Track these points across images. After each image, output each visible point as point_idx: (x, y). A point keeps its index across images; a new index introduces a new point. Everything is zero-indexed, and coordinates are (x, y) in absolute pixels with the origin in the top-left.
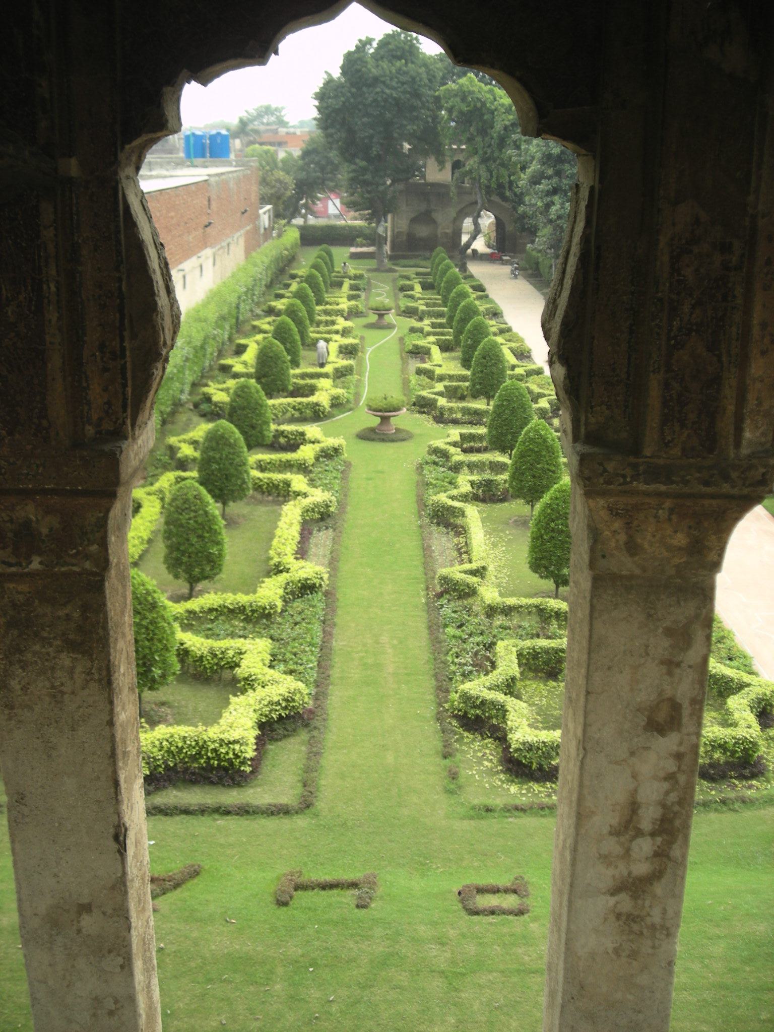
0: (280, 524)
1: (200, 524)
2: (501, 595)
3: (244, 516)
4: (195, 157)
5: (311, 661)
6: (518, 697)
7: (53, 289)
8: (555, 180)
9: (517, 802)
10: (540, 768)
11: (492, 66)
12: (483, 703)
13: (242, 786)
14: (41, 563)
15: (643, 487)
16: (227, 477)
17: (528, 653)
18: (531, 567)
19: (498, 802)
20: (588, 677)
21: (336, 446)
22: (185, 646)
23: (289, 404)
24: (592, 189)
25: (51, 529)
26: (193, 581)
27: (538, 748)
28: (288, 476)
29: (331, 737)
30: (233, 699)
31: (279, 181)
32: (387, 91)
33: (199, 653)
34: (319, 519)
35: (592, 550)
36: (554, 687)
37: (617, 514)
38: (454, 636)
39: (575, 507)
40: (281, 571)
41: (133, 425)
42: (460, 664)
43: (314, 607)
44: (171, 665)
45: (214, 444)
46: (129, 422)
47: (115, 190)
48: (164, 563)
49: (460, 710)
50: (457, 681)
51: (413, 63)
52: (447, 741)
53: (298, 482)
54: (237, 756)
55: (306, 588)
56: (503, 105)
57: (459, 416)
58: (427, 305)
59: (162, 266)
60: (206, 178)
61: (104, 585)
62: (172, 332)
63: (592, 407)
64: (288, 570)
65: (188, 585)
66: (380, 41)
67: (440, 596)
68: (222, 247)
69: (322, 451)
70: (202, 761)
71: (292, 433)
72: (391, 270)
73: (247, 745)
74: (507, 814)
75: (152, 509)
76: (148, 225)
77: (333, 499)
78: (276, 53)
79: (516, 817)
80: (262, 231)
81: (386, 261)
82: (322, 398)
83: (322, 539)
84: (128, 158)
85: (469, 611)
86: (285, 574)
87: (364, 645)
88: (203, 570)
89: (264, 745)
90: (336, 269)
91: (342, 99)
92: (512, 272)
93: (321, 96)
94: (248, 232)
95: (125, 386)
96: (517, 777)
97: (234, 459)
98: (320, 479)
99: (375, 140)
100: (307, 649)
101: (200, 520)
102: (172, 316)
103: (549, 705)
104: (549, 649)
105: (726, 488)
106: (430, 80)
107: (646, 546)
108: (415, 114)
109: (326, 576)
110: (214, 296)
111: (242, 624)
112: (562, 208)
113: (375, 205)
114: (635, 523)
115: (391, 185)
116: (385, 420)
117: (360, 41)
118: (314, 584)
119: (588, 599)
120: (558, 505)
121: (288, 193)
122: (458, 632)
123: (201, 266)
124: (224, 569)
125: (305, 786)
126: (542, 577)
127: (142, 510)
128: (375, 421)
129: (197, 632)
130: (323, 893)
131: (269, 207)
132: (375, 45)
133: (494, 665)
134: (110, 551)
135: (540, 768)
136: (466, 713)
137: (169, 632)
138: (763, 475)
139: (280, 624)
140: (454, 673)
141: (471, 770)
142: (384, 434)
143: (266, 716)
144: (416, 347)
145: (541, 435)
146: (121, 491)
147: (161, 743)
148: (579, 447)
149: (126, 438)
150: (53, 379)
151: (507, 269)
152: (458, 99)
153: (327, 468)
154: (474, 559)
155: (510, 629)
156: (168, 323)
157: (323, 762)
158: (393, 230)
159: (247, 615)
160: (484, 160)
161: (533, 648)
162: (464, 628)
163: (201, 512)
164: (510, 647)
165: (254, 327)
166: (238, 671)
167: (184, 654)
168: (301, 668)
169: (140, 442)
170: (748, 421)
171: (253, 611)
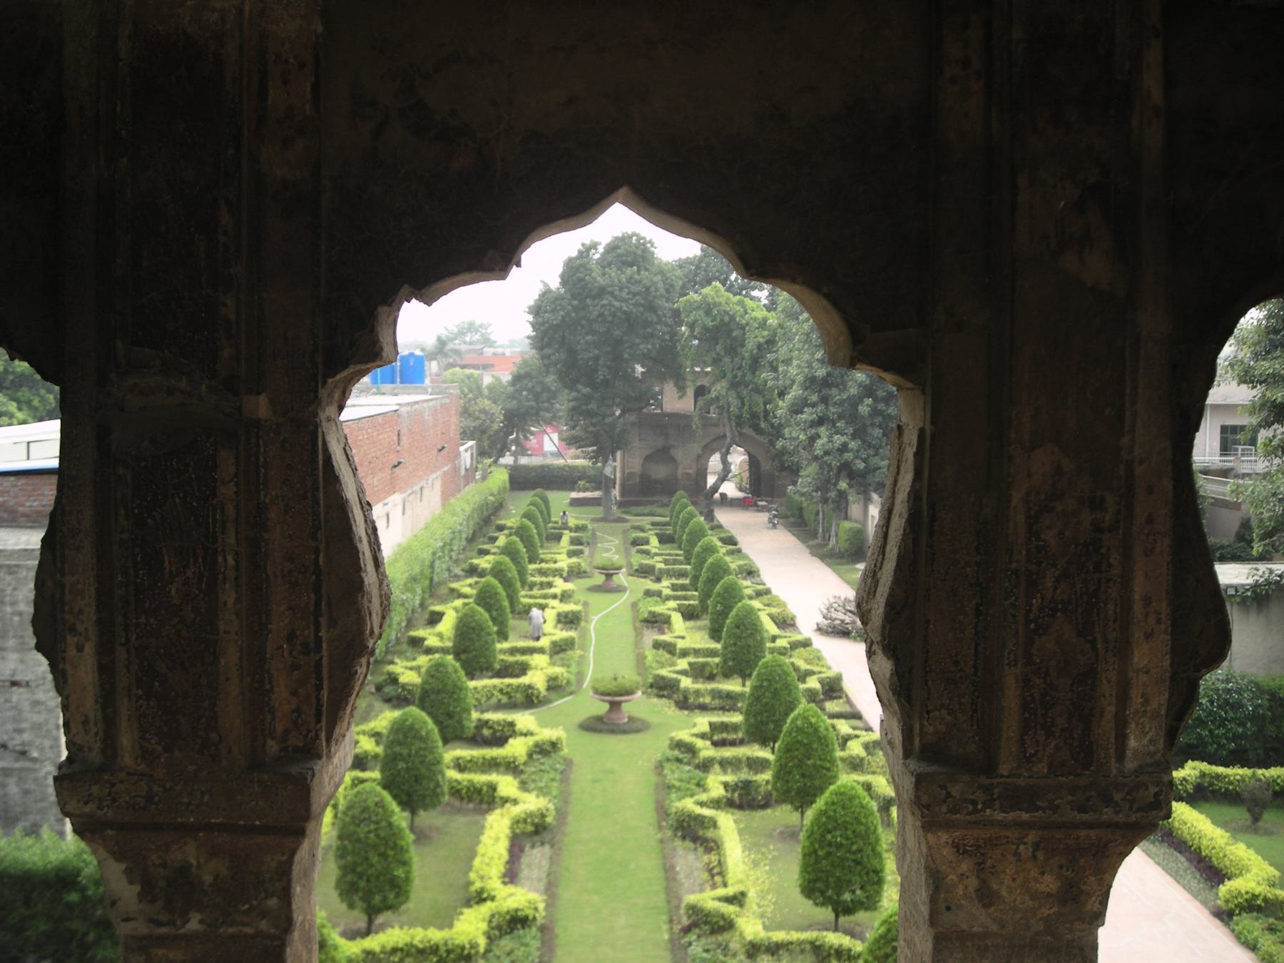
0: (484, 838)
1: (384, 838)
2: (766, 928)
3: (437, 829)
7: (231, 561)
8: (821, 408)
11: (793, 280)
14: (201, 922)
15: (1000, 816)
16: (417, 779)
18: (803, 892)
21: (554, 739)
23: (495, 687)
24: (922, 433)
25: (217, 876)
26: (372, 912)
28: (493, 777)
31: (486, 413)
32: (617, 304)
34: (532, 833)
35: (933, 900)
37: (965, 851)
40: (484, 900)
41: (329, 739)
43: (526, 945)
45: (401, 737)
46: (323, 735)
51: (646, 270)
53: (506, 785)
55: (516, 922)
56: (755, 319)
57: (707, 700)
59: (370, 532)
63: (928, 712)
64: (493, 899)
67: (687, 930)
69: (537, 745)
71: (498, 723)
77: (551, 806)
78: (518, 265)
80: (463, 472)
81: (615, 508)
82: (536, 678)
83: (536, 857)
84: (331, 395)
85: (725, 949)
86: (489, 904)
88: (385, 899)
90: (553, 519)
92: (770, 521)
93: (537, 310)
94: (445, 473)
95: (319, 688)
98: (534, 781)
99: (601, 362)
101: (382, 834)
102: (381, 596)
105: (1107, 814)
106: (668, 291)
107: (1004, 893)
108: (649, 330)
113: (603, 442)
114: (989, 863)
115: (620, 416)
116: (615, 706)
117: (583, 245)
120: (835, 811)
121: (495, 427)
124: (413, 896)
126: (817, 904)
128: (602, 708)
131: (471, 443)
132: (601, 249)
134: (294, 907)
138: (1156, 795)
144: (653, 614)
146: (311, 826)
148: (913, 764)
149: (320, 757)
150: (227, 679)
151: (764, 517)
152: (701, 312)
154: (730, 882)
158: (623, 472)
160: (734, 385)
165: (452, 590)
169: (336, 760)
170: (1133, 725)
171: (449, 952)
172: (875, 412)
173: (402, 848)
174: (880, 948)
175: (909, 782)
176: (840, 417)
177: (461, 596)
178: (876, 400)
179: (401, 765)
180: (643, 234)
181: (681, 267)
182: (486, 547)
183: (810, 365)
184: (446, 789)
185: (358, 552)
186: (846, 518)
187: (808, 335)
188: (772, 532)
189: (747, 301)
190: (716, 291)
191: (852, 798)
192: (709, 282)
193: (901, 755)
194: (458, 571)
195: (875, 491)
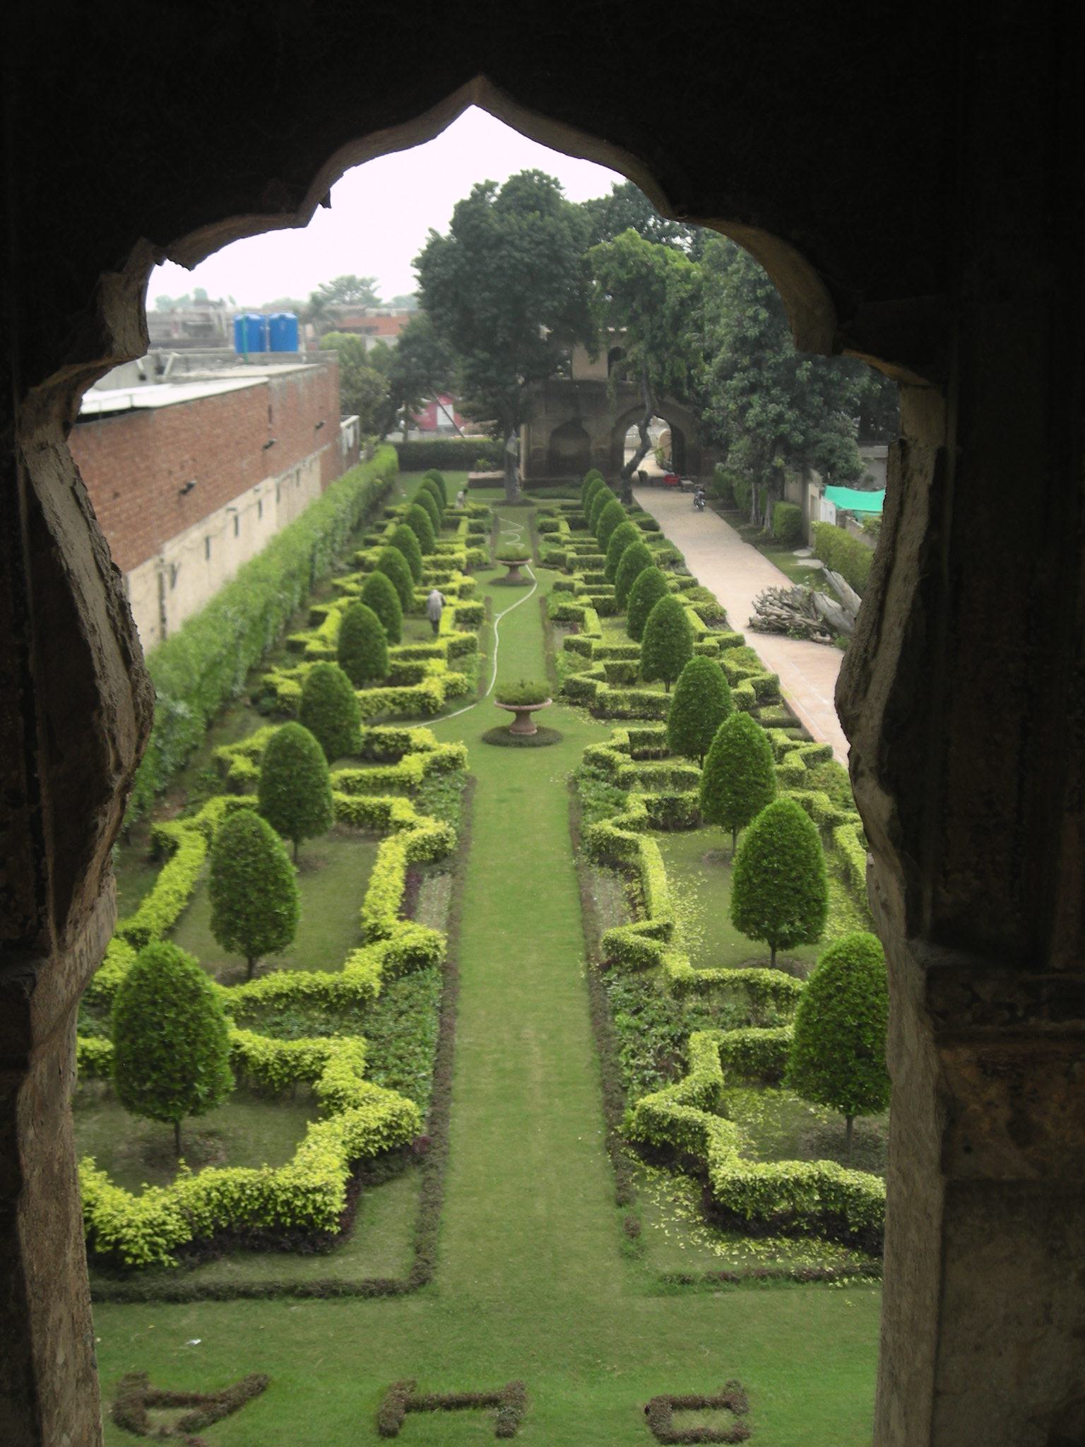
0: (377, 869)
1: (262, 873)
2: (694, 964)
3: (324, 858)
4: (250, 350)
5: (424, 1068)
6: (723, 1114)
8: (752, 373)
9: (726, 1268)
10: (758, 1217)
11: (746, 221)
12: (674, 1123)
13: (327, 1255)
15: (1047, 1025)
16: (300, 804)
17: (735, 1049)
18: (735, 924)
19: (698, 1269)
20: (937, 1363)
21: (454, 754)
22: (242, 1049)
23: (386, 696)
24: (941, 456)
26: (253, 954)
27: (754, 1189)
28: (387, 799)
29: (455, 1180)
30: (312, 1127)
31: (367, 381)
32: (517, 255)
33: (262, 1060)
34: (430, 861)
35: (946, 1139)
36: (774, 1097)
38: (628, 1027)
39: (900, 1037)
40: (379, 938)
41: (60, 926)
42: (638, 1067)
43: (426, 988)
44: (222, 1079)
45: (280, 756)
46: (51, 922)
47: (11, 475)
48: (212, 929)
49: (639, 1135)
50: (634, 1092)
51: (551, 215)
52: (622, 1180)
53: (401, 808)
54: (318, 1211)
55: (414, 961)
56: (677, 271)
57: (627, 707)
58: (578, 551)
59: (114, 613)
60: (266, 379)
62: (135, 738)
64: (388, 936)
65: (246, 961)
66: (505, 186)
67: (606, 968)
68: (289, 476)
70: (269, 1219)
71: (391, 737)
72: (526, 503)
73: (334, 1193)
74: (712, 1287)
75: (192, 850)
76: (85, 535)
77: (451, 830)
78: (326, 204)
79: (725, 1291)
80: (345, 452)
81: (519, 490)
82: (433, 686)
83: (436, 888)
85: (649, 988)
86: (384, 942)
88: (266, 938)
89: (358, 1192)
90: (450, 504)
91: (454, 266)
92: (696, 502)
93: (425, 263)
95: (39, 854)
96: (724, 1231)
97: (308, 778)
98: (432, 802)
99: (500, 322)
100: (418, 1050)
101: (261, 866)
102: (136, 705)
103: (766, 1122)
104: (764, 1042)
106: (575, 239)
108: (555, 285)
110: (278, 545)
111: (323, 1016)
112: (764, 411)
115: (524, 384)
116: (522, 716)
117: (477, 186)
118: (426, 956)
119: (936, 1222)
120: (771, 834)
121: (381, 399)
122: (634, 1021)
123: (260, 504)
124: (297, 935)
125: (418, 1252)
126: (751, 938)
127: (179, 852)
128: (508, 718)
129: (258, 1029)
130: (447, 1414)
131: (354, 418)
132: (498, 191)
133: (687, 1069)
134: (24, 1160)
135: (758, 1217)
136: (648, 1139)
137: (218, 1031)
139: (378, 1014)
140: (630, 1080)
141: (658, 1222)
142: (521, 736)
143: (360, 1150)
145: (744, 734)
147: (209, 1194)
149: (46, 952)
151: (689, 498)
152: (615, 264)
153: (442, 787)
154: (654, 913)
155: (708, 1014)
156: (124, 723)
157: (444, 1216)
158: (528, 448)
159: (331, 1002)
160: (653, 348)
161: (743, 1042)
162: (642, 1014)
163: (262, 856)
164: (709, 1041)
165: (336, 587)
166: (318, 1085)
167: (241, 1060)
168: (409, 1078)
169: (79, 945)
171: (339, 997)
172: (815, 377)
173: (284, 881)
174: (822, 989)
176: (776, 383)
177: (346, 593)
179: (282, 788)
180: (546, 173)
181: (590, 211)
182: (373, 537)
183: (740, 324)
185: (88, 650)
186: (783, 499)
187: (737, 288)
188: (699, 516)
189: (668, 250)
190: (629, 238)
191: (791, 819)
192: (622, 228)
193: (903, 930)
195: (815, 468)
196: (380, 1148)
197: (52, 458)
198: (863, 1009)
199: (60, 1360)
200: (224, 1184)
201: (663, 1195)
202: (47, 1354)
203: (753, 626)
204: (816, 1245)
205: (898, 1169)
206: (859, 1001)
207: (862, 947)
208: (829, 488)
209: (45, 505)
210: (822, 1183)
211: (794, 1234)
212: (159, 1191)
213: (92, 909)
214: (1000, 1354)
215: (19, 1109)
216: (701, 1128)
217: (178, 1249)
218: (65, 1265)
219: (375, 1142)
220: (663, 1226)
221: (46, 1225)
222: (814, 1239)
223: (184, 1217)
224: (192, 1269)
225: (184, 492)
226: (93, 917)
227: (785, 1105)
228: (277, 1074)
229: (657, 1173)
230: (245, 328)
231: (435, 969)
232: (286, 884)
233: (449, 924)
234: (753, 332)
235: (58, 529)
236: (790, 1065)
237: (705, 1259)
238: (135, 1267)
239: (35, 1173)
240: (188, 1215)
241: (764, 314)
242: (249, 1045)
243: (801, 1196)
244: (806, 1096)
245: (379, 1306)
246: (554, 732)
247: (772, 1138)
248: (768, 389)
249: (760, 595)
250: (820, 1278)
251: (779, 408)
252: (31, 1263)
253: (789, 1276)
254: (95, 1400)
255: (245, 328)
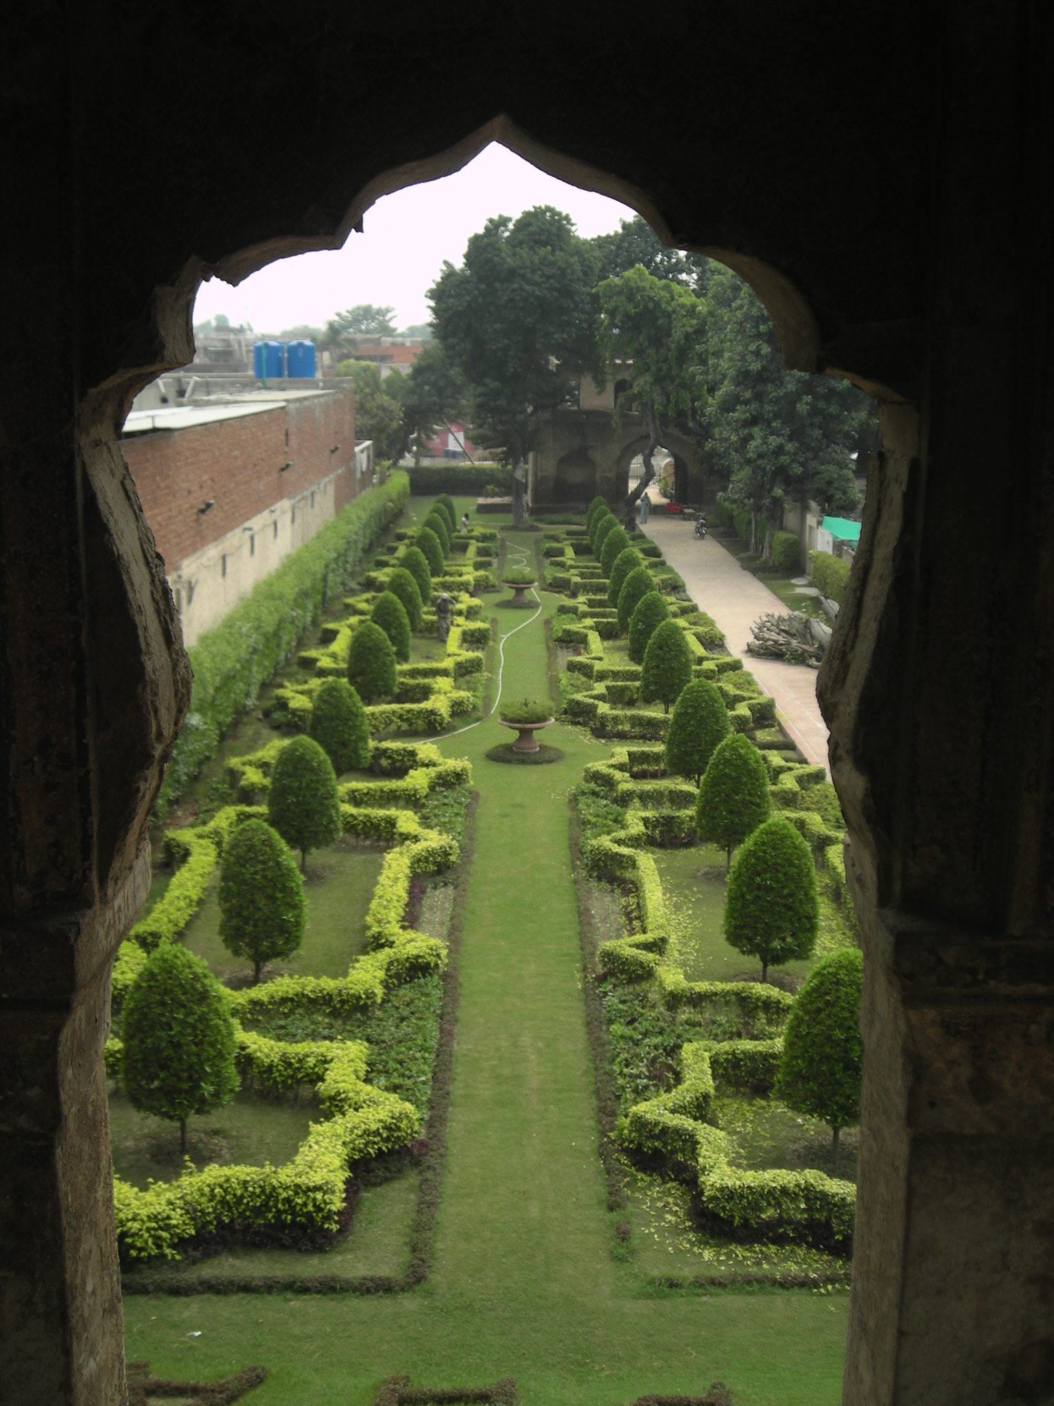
0: (381, 879)
1: (271, 880)
2: (688, 977)
3: (331, 868)
4: (268, 376)
5: (424, 1073)
6: (713, 1123)
9: (714, 1273)
10: (746, 1224)
11: (739, 249)
12: (665, 1130)
13: (326, 1252)
16: (309, 814)
17: (726, 1060)
18: (728, 939)
19: (687, 1273)
20: (902, 1305)
21: (459, 769)
22: (248, 1051)
24: (914, 466)
26: (259, 959)
27: (742, 1196)
28: (392, 812)
29: (451, 1181)
30: (314, 1128)
31: (382, 408)
32: (528, 288)
33: (267, 1061)
34: (432, 872)
35: (912, 1094)
36: (763, 1108)
38: (622, 1037)
39: (873, 1003)
40: (382, 946)
41: (103, 880)
42: (631, 1076)
43: (427, 995)
45: (291, 769)
46: (94, 876)
47: (69, 466)
48: (220, 934)
49: (631, 1142)
50: (626, 1100)
51: (561, 250)
52: (614, 1185)
53: (407, 821)
54: (318, 1209)
55: (416, 969)
56: (683, 306)
57: (627, 727)
58: (582, 575)
60: (283, 404)
61: (52, 1154)
62: (174, 711)
65: (253, 965)
66: (518, 221)
67: (602, 979)
68: (304, 498)
69: (439, 776)
70: (270, 1215)
71: (397, 752)
73: (333, 1192)
74: (700, 1291)
76: (133, 525)
78: (359, 229)
79: (711, 1295)
80: (359, 475)
81: (526, 515)
82: (439, 704)
83: (439, 899)
85: (644, 1000)
86: (387, 949)
87: (498, 1049)
88: (274, 944)
89: (357, 1192)
92: (698, 530)
94: (339, 477)
96: (712, 1237)
98: (435, 816)
99: (511, 353)
100: (418, 1055)
101: (270, 874)
102: (175, 682)
103: (755, 1132)
106: (585, 273)
108: (565, 318)
109: (444, 952)
110: (292, 564)
111: (327, 1020)
116: (525, 734)
117: (491, 221)
118: (428, 964)
119: (903, 1173)
120: (765, 852)
121: (394, 425)
122: (628, 1031)
123: (275, 524)
124: (304, 941)
125: (414, 1251)
126: (743, 952)
127: (191, 859)
128: (512, 736)
129: (264, 1032)
131: (368, 443)
132: (511, 226)
133: (678, 1079)
134: (63, 1097)
135: (746, 1224)
136: (640, 1145)
137: (224, 1032)
139: (381, 1020)
140: (623, 1088)
141: (648, 1226)
143: (360, 1151)
144: (567, 632)
147: (212, 1190)
149: (89, 904)
151: (691, 526)
152: (623, 298)
153: (446, 801)
154: (650, 927)
155: (700, 1025)
157: (440, 1216)
158: (535, 475)
159: (334, 1007)
160: (658, 380)
162: (636, 1024)
163: (271, 864)
164: (701, 1052)
165: (347, 606)
167: (246, 1062)
168: (409, 1082)
169: (118, 902)
171: (343, 1002)
172: (814, 411)
174: (811, 1002)
175: (884, 942)
178: (816, 397)
179: (291, 799)
180: (558, 209)
181: (600, 246)
182: (384, 558)
183: (743, 359)
184: (340, 825)
185: (135, 627)
186: (782, 528)
187: (741, 324)
188: (700, 543)
189: (674, 285)
190: (637, 273)
192: (631, 265)
193: (874, 900)
194: (353, 585)
196: (380, 1149)
197: (105, 455)
198: (852, 1023)
199: (89, 1288)
200: (228, 1180)
201: (653, 1200)
202: (78, 1281)
203: (751, 651)
204: (801, 1252)
205: (870, 1129)
206: (847, 1015)
207: (851, 962)
208: (827, 519)
209: (99, 497)
210: (810, 1194)
211: (780, 1241)
212: (164, 1186)
213: (131, 868)
214: (961, 1298)
215: (60, 1049)
216: (692, 1136)
217: (181, 1243)
218: (96, 1201)
219: (374, 1143)
220: (652, 1230)
221: (81, 1162)
222: (799, 1246)
223: (187, 1212)
224: (194, 1262)
225: (203, 511)
226: (131, 878)
227: (774, 1116)
228: (281, 1075)
229: (648, 1179)
230: (264, 355)
231: (436, 977)
232: (291, 892)
233: (450, 934)
234: (755, 366)
235: (111, 518)
236: (780, 1076)
237: (693, 1264)
238: (138, 1259)
239: (74, 1110)
240: (191, 1210)
241: (766, 349)
242: (254, 1047)
243: (787, 1204)
244: (795, 1107)
245: (375, 1302)
246: (556, 749)
247: (761, 1147)
248: (769, 422)
249: (758, 621)
250: (805, 1284)
251: (780, 440)
252: (66, 1195)
253: (774, 1282)
254: (119, 1331)
255: (264, 355)
